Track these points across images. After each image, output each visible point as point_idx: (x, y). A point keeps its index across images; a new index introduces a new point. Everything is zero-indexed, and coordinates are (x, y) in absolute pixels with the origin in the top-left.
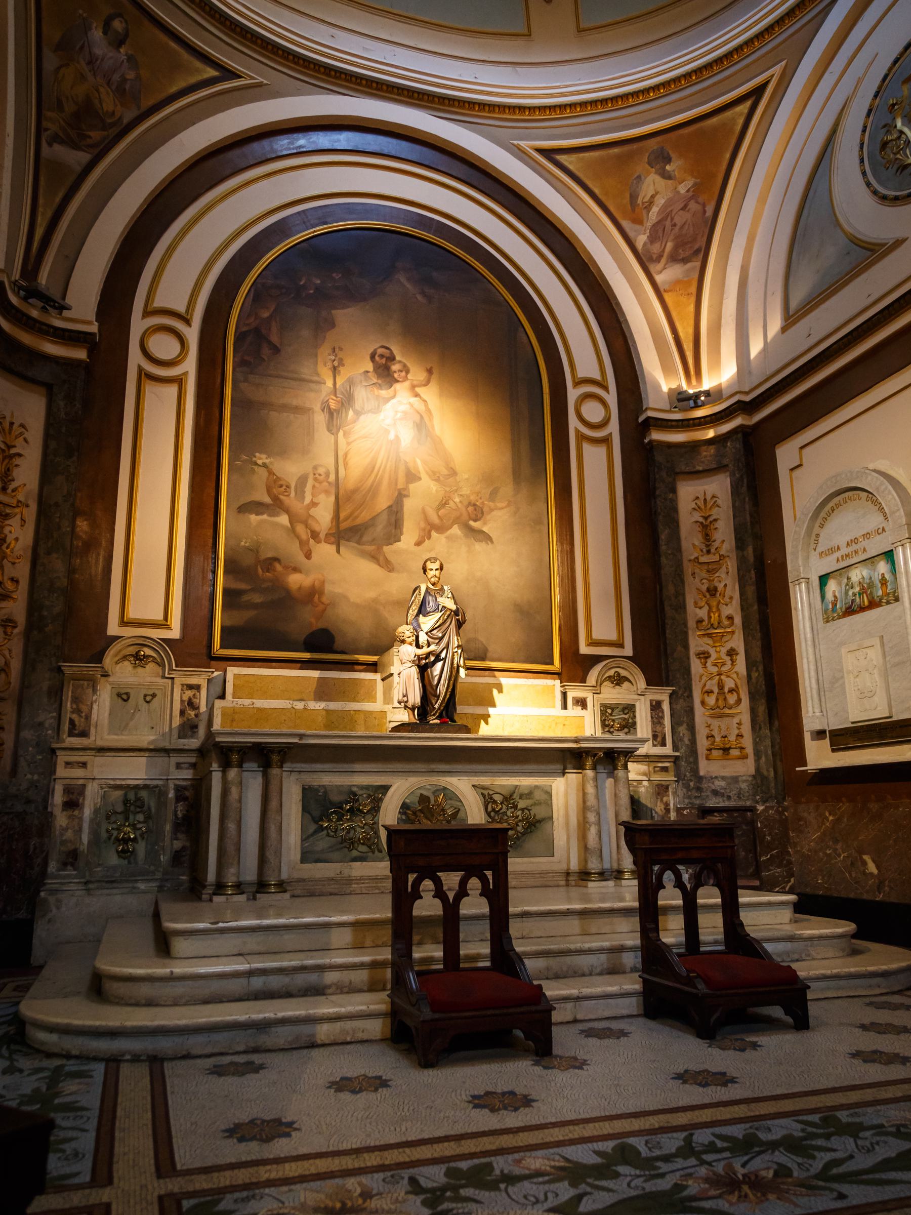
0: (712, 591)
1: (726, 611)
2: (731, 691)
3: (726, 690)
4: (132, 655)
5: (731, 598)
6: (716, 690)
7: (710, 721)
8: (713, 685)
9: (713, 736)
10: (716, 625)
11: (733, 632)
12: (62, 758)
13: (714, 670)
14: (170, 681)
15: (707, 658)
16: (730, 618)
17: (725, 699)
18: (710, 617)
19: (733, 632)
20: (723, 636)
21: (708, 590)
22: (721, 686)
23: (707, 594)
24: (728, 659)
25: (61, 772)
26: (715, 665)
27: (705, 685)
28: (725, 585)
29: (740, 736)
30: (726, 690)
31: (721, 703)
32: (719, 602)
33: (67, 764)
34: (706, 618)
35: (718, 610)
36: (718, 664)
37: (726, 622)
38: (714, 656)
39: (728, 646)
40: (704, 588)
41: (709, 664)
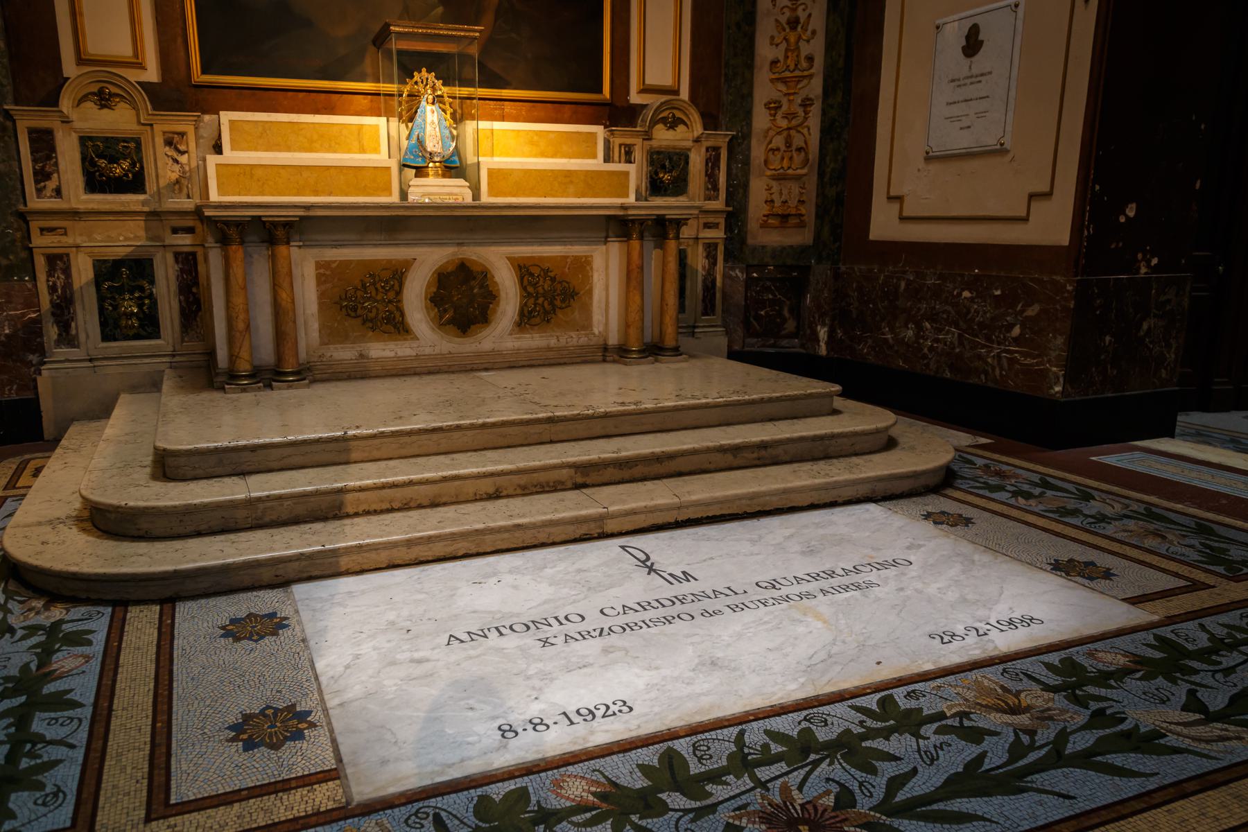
0: (794, 23)
1: (805, 49)
2: (799, 150)
3: (794, 147)
4: (93, 94)
5: (814, 32)
6: (783, 148)
7: (774, 184)
8: (779, 141)
9: (772, 201)
10: (792, 67)
11: (811, 76)
12: (35, 225)
13: (784, 124)
14: (148, 128)
15: (776, 108)
16: (810, 59)
17: (791, 158)
18: (786, 57)
19: (811, 76)
20: (799, 82)
21: (789, 23)
22: (788, 144)
23: (787, 27)
24: (800, 112)
25: (38, 241)
26: (785, 117)
27: (770, 142)
28: (810, 15)
29: (802, 202)
30: (794, 147)
31: (785, 163)
32: (800, 38)
33: (42, 230)
34: (781, 58)
35: (798, 48)
36: (790, 116)
37: (804, 64)
38: (785, 108)
39: (803, 94)
40: (783, 19)
41: (778, 117)
